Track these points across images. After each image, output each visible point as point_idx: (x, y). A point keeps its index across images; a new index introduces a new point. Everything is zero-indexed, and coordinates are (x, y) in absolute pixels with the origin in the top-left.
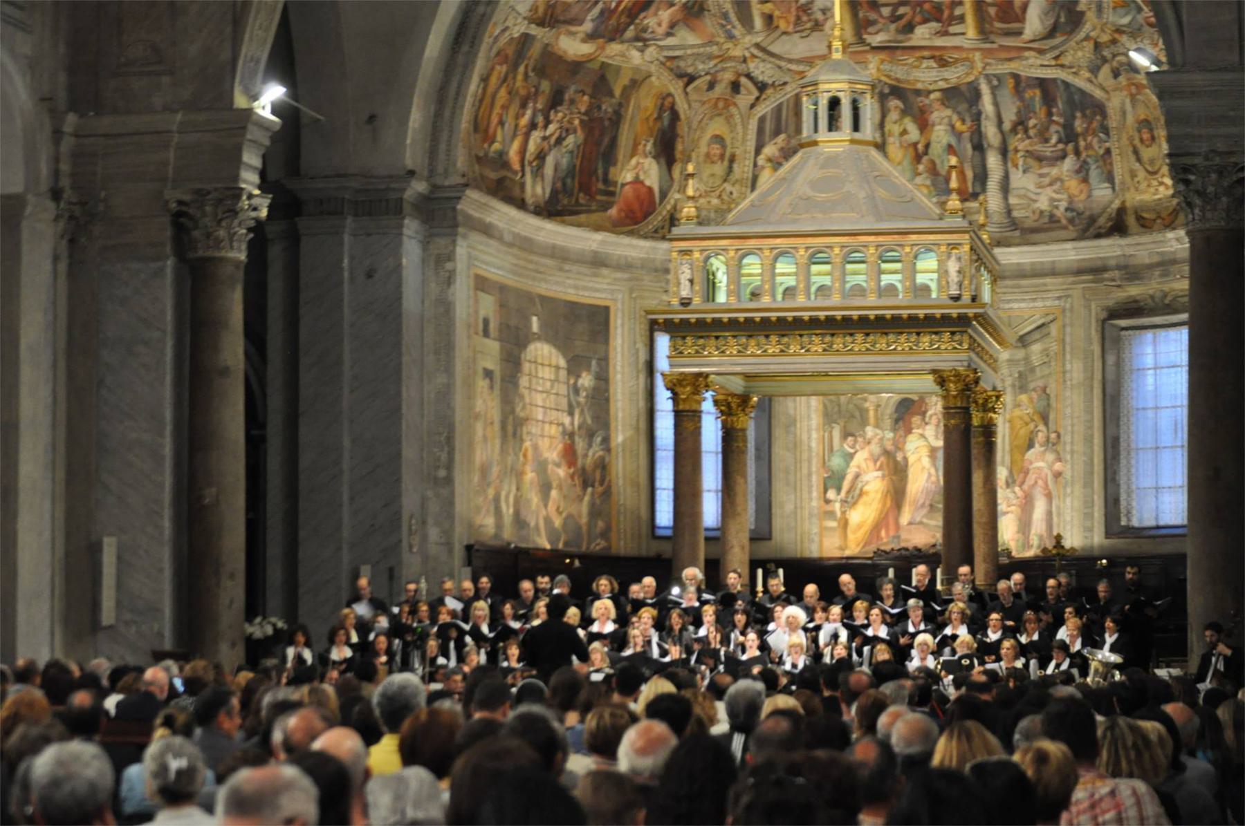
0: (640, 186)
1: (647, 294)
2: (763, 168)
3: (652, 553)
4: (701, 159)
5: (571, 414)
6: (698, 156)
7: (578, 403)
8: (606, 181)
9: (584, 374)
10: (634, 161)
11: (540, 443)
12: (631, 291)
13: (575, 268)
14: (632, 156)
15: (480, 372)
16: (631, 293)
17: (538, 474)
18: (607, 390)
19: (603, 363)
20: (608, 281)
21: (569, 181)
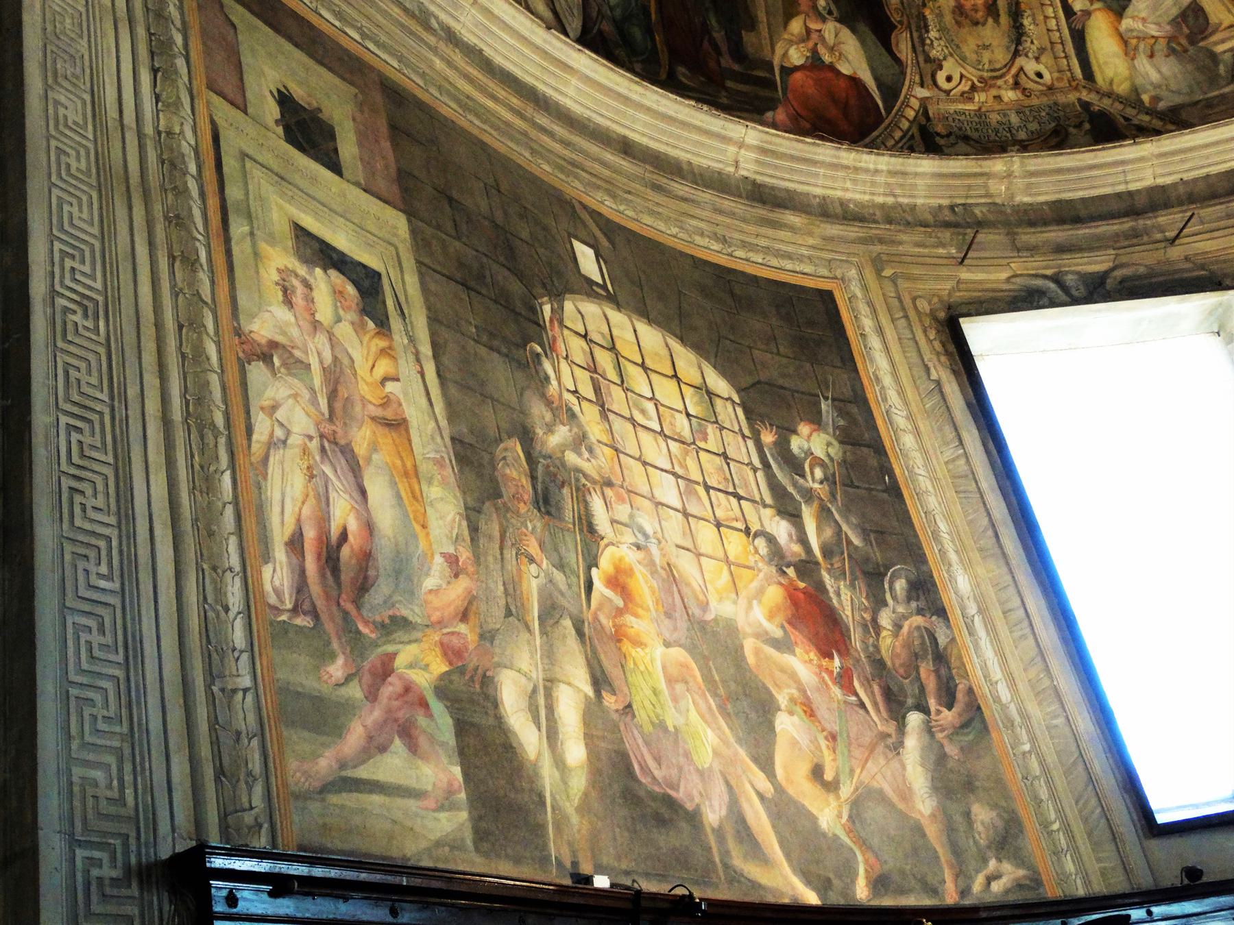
0: (830, 75)
1: (916, 271)
2: (1087, 14)
3: (1171, 877)
4: (948, 19)
5: (788, 509)
6: (940, 15)
7: (809, 495)
8: (738, 53)
9: (804, 429)
10: (796, 26)
11: (686, 564)
12: (878, 264)
13: (706, 196)
14: (789, 16)
15: (281, 227)
16: (878, 273)
17: (692, 650)
18: (886, 469)
19: (854, 410)
20: (811, 241)
21: (637, 33)
